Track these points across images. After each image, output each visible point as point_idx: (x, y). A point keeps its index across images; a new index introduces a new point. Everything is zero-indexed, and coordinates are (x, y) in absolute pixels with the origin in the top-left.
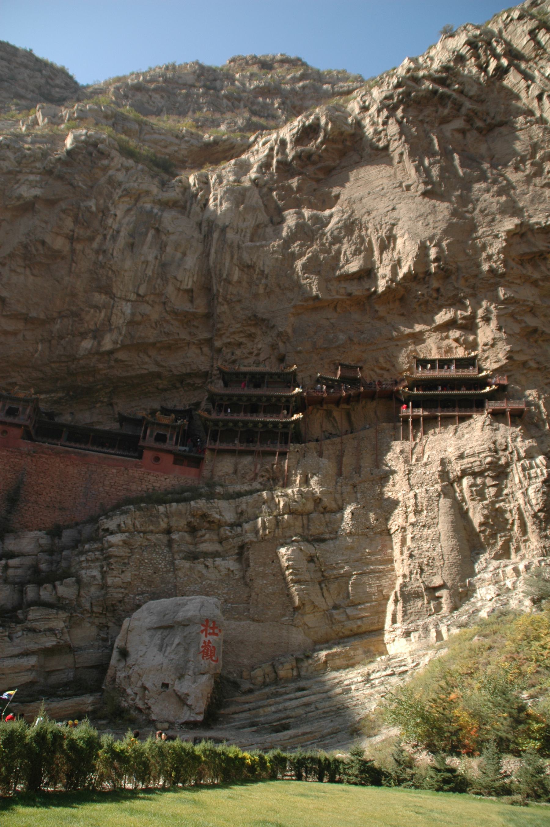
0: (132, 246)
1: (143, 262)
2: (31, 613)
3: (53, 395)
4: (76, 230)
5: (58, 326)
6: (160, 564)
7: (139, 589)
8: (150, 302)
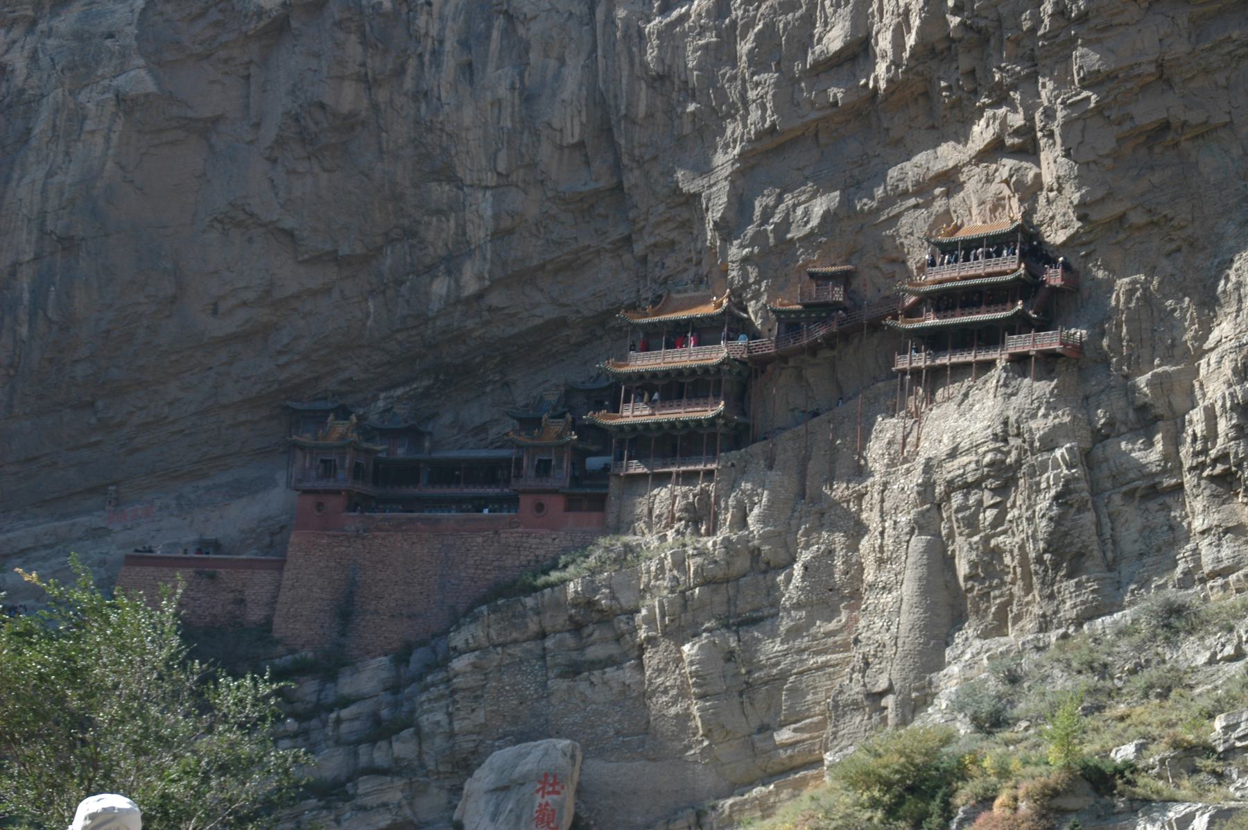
0: (468, 70)
2: (360, 785)
3: (415, 386)
4: (369, 61)
5: (389, 261)
6: (527, 689)
8: (520, 184)
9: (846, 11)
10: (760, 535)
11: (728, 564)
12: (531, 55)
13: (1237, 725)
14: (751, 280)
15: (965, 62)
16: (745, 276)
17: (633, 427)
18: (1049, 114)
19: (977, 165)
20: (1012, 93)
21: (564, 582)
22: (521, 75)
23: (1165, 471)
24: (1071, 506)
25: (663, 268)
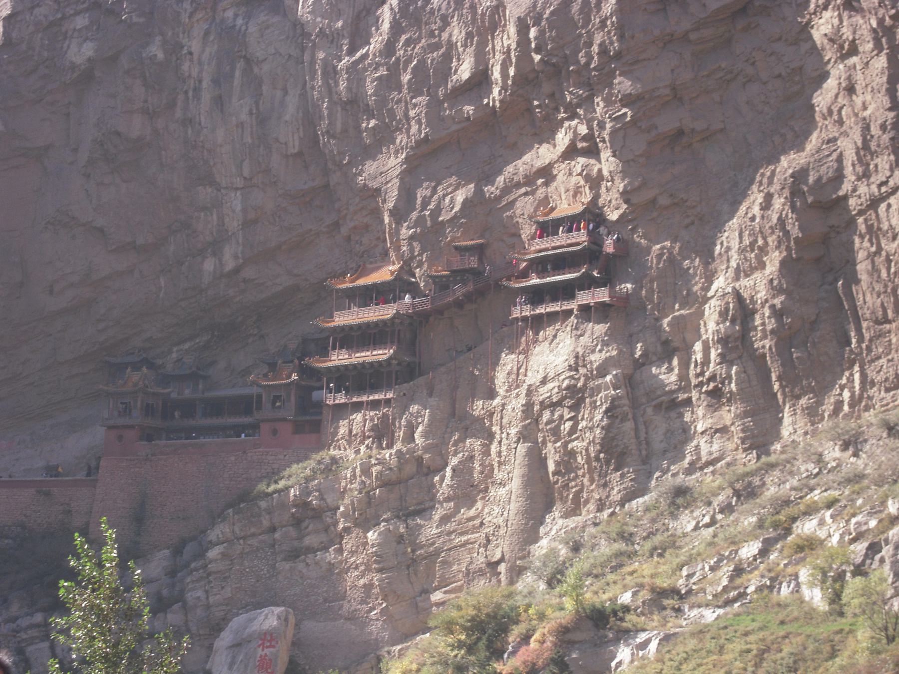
0: (219, 102)
1: (237, 126)
3: (197, 341)
6: (262, 570)
7: (243, 602)
9: (470, 50)
10: (423, 447)
11: (400, 469)
12: (264, 88)
13: (694, 574)
14: (416, 253)
15: (547, 88)
16: (412, 250)
17: (337, 368)
18: (602, 125)
19: (563, 162)
20: (578, 110)
21: (287, 489)
22: (257, 103)
23: (680, 389)
24: (617, 417)
25: (361, 245)
